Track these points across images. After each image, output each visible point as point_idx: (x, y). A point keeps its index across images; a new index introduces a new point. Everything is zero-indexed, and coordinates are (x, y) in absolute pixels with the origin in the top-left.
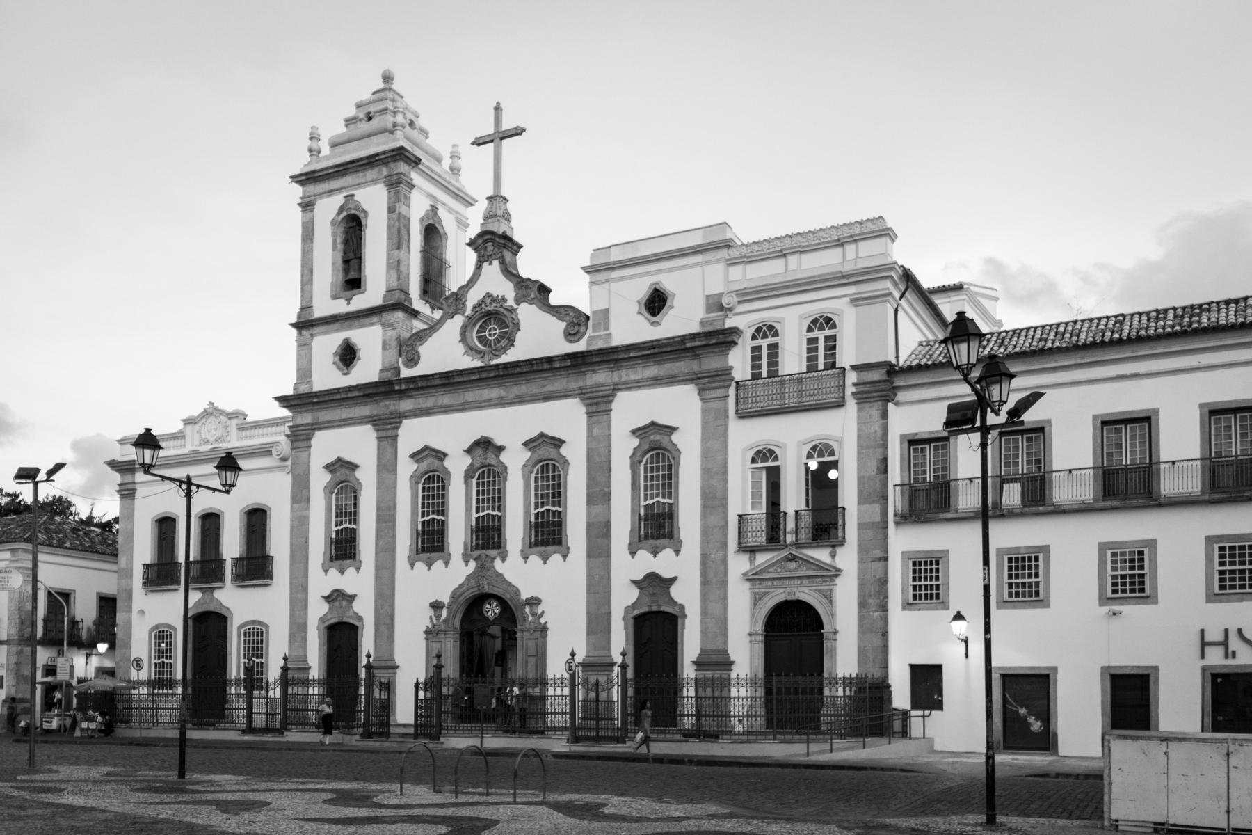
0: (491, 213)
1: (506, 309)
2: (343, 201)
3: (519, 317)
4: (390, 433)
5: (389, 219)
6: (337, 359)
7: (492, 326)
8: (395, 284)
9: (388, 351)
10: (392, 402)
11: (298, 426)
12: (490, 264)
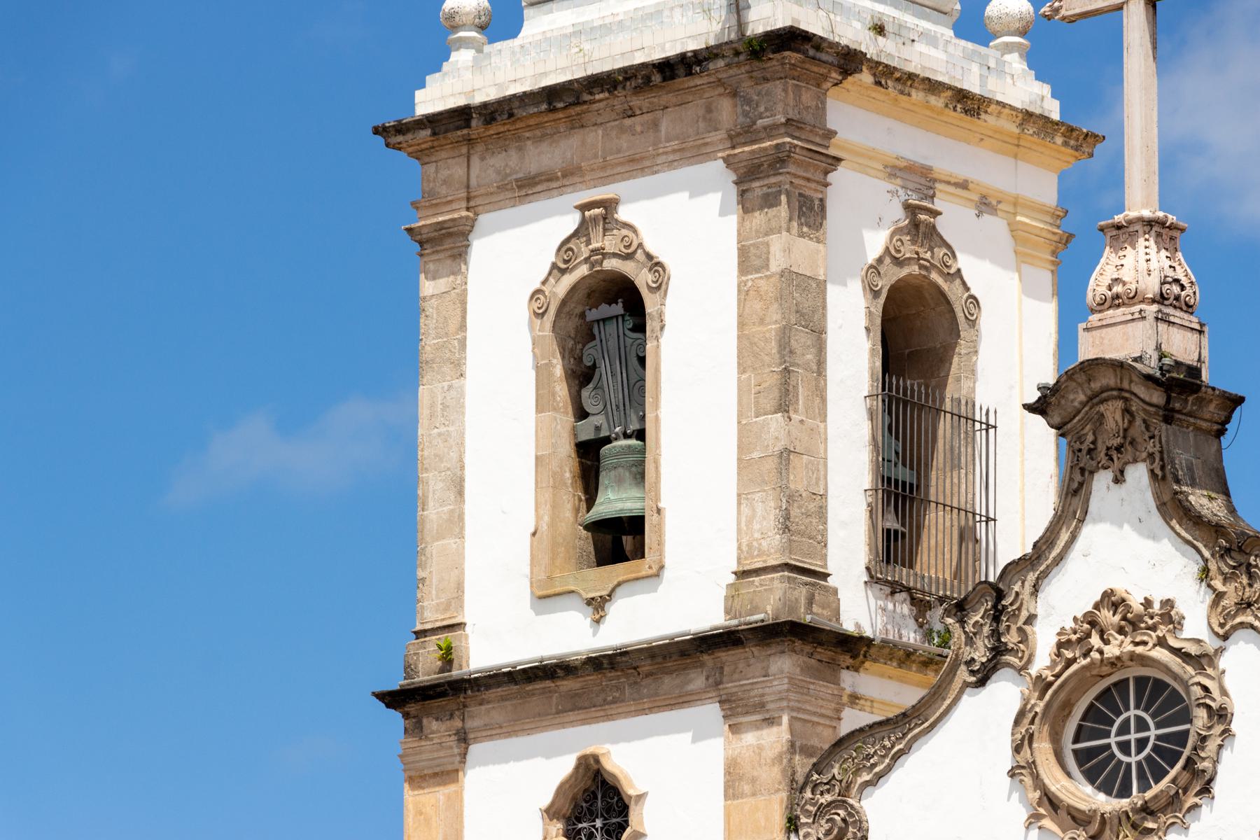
0: (1118, 289)
1: (1177, 652)
2: (571, 222)
3: (1228, 682)
5: (744, 294)
7: (1132, 712)
8: (772, 549)
9: (748, 803)
12: (1119, 479)
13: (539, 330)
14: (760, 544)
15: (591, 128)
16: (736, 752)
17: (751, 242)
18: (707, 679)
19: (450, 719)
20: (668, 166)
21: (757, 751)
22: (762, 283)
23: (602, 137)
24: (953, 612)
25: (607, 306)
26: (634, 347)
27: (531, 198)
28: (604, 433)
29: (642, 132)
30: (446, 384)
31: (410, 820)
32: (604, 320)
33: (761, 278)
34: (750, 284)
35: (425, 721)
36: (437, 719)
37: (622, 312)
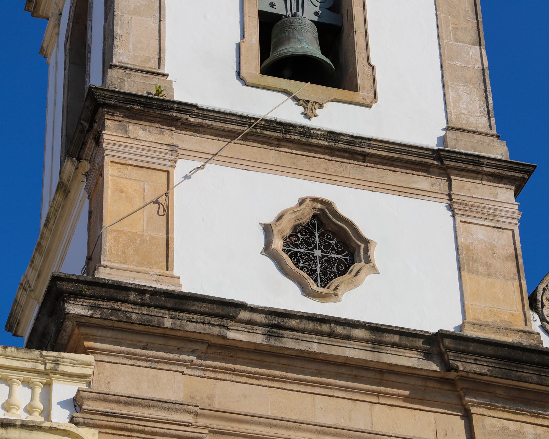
6: (278, 244)
14: (468, 118)
16: (468, 242)
28: (280, 10)
36: (144, 130)
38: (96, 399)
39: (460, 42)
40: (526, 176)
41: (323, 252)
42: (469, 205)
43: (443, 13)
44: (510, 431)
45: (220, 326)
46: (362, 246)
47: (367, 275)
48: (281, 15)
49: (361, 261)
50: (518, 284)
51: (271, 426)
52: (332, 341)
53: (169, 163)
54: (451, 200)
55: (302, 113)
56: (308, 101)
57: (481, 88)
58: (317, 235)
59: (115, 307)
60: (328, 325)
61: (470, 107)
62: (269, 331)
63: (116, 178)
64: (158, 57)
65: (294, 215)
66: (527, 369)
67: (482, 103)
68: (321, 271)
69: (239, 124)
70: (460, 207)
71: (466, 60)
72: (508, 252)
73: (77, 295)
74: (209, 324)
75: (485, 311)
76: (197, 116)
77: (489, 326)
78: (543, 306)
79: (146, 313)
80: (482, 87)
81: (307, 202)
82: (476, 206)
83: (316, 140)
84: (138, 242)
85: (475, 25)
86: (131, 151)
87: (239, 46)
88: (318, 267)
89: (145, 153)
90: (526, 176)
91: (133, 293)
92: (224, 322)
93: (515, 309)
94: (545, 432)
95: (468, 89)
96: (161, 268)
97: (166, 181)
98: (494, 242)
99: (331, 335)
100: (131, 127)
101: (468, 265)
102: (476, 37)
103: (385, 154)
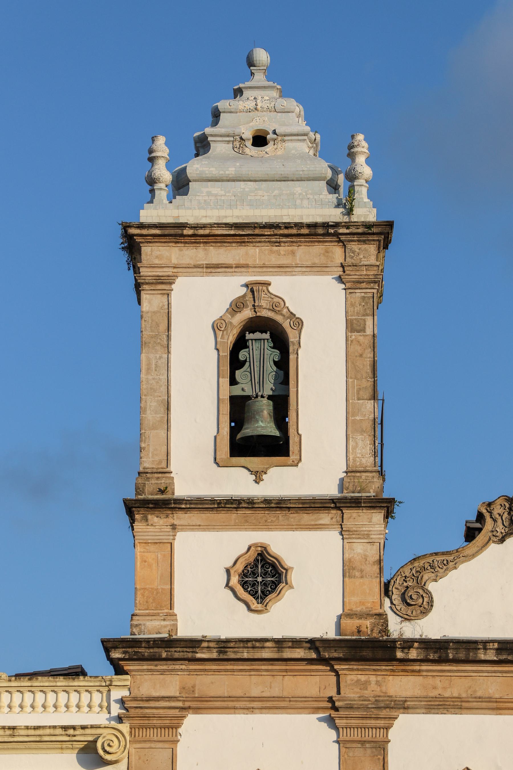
4: (369, 735)
6: (235, 580)
9: (358, 582)
10: (373, 678)
11: (149, 699)
13: (221, 338)
14: (361, 460)
15: (251, 247)
16: (351, 556)
17: (354, 317)
18: (332, 519)
19: (166, 518)
20: (302, 274)
21: (364, 557)
22: (361, 338)
23: (259, 253)
24: (484, 507)
25: (260, 334)
26: (272, 356)
27: (214, 274)
28: (248, 392)
29: (285, 255)
30: (158, 356)
31: (138, 564)
32: (255, 340)
33: (361, 335)
34: (353, 337)
35: (149, 517)
36: (157, 517)
37: (269, 337)
38: (131, 700)
39: (361, 400)
40: (389, 505)
41: (263, 578)
42: (352, 531)
43: (351, 378)
44: (362, 682)
45: (193, 652)
46: (284, 571)
47: (286, 591)
48: (249, 396)
49: (283, 583)
50: (379, 580)
51: (224, 701)
52: (255, 650)
53: (172, 537)
54: (342, 528)
55: (254, 480)
56: (258, 471)
57: (372, 434)
58: (260, 567)
59: (136, 650)
60: (251, 643)
61: (364, 451)
62: (219, 650)
63: (142, 553)
64: (166, 459)
65: (244, 559)
66: (366, 650)
67: (371, 446)
68: (261, 591)
69: (211, 504)
70: (347, 533)
71: (364, 413)
72: (376, 558)
73: (115, 648)
74: (186, 652)
75: (357, 603)
76: (186, 504)
77: (356, 614)
78: (393, 593)
79: (152, 651)
80: (373, 433)
81: (252, 548)
82: (357, 531)
83: (258, 505)
84: (155, 593)
85: (373, 383)
86: (150, 534)
87: (215, 437)
88: (259, 588)
89: (158, 534)
90: (389, 505)
91: (143, 642)
92: (194, 650)
93: (376, 598)
94: (382, 679)
95: (363, 437)
96: (167, 609)
97: (170, 549)
98: (367, 553)
99: (254, 647)
100: (149, 517)
101: (349, 573)
102: (372, 393)
103: (301, 506)
